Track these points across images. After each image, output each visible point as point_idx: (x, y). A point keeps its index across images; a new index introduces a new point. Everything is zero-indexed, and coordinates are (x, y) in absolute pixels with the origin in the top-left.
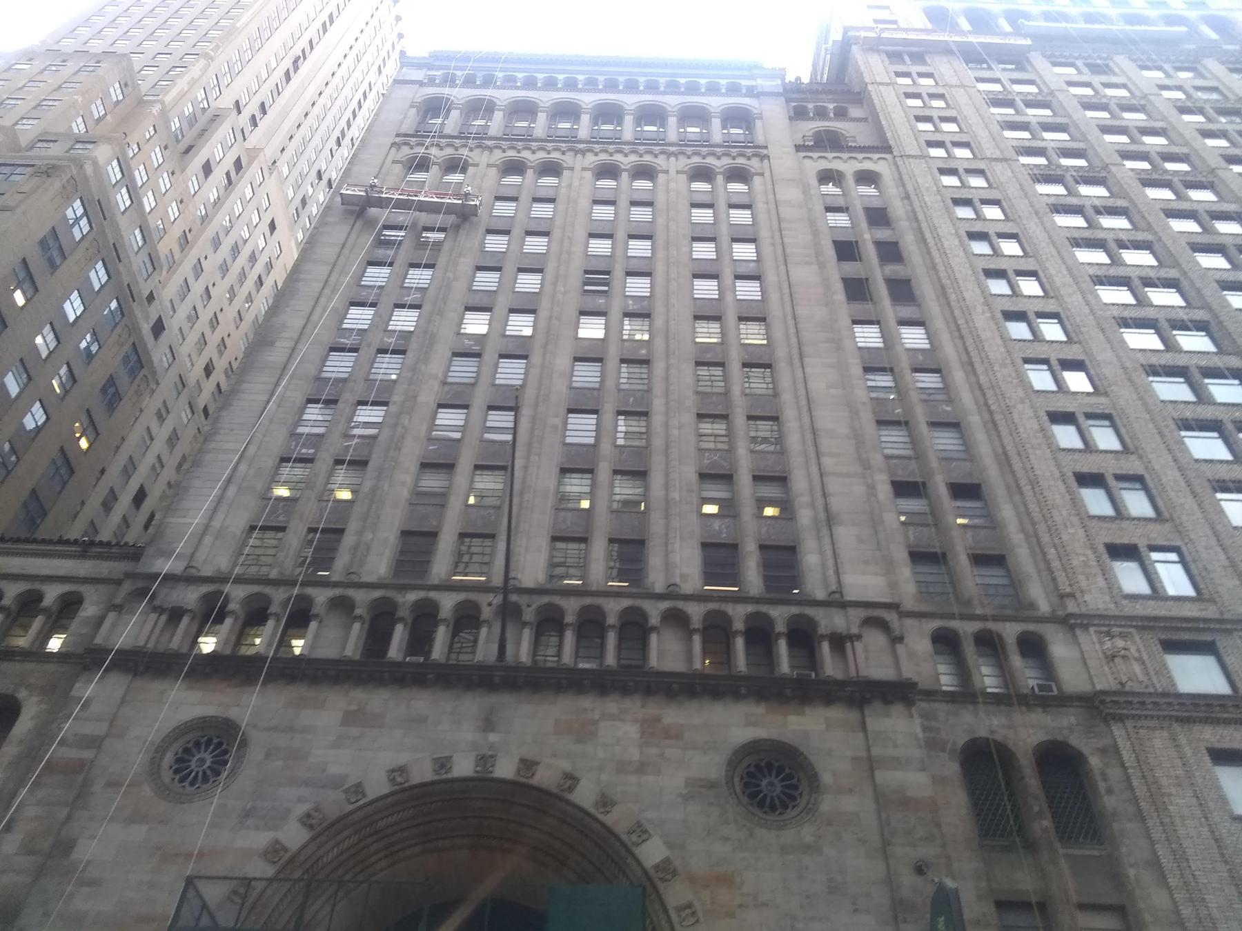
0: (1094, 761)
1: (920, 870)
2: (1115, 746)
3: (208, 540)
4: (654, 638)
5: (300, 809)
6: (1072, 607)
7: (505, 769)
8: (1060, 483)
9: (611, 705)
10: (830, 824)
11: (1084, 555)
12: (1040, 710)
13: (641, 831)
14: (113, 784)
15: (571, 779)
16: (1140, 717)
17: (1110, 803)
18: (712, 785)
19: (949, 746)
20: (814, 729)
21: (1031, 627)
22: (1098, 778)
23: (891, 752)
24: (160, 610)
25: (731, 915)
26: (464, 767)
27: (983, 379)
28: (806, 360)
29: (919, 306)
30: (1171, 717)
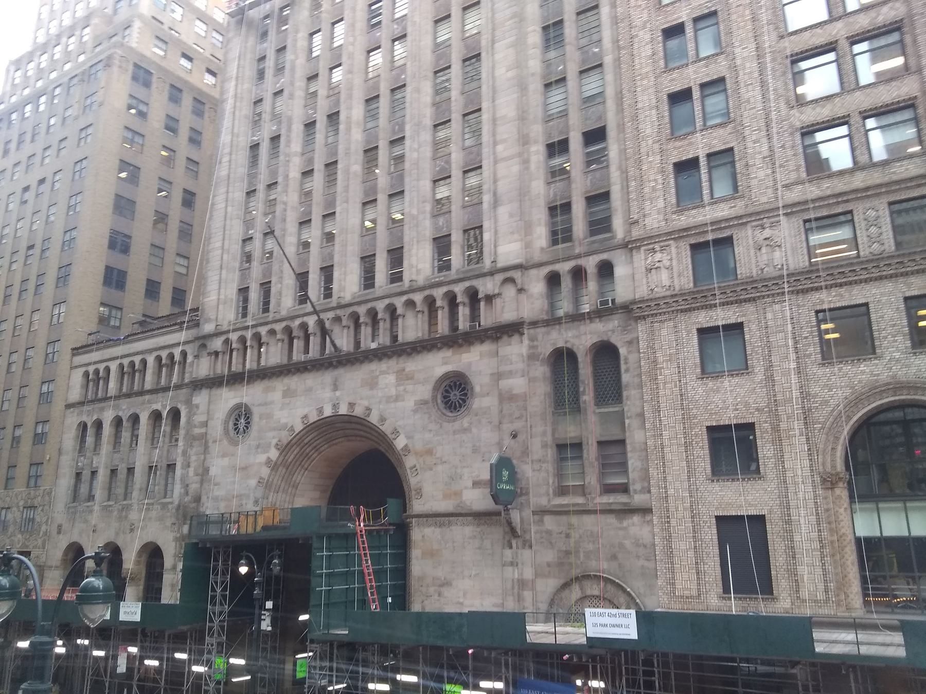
0: (623, 351)
1: (515, 436)
2: (638, 338)
3: (221, 307)
4: (400, 320)
5: (274, 441)
6: (636, 233)
7: (343, 410)
8: (654, 112)
9: (384, 365)
10: (476, 415)
11: (655, 180)
12: (598, 320)
13: (396, 432)
14: (215, 441)
15: (369, 409)
16: (656, 315)
17: (625, 378)
18: (425, 402)
19: (541, 356)
20: (474, 361)
21: (604, 256)
22: (622, 362)
23: (508, 368)
24: (209, 354)
25: (431, 469)
26: (328, 412)
28: (496, 45)
30: (677, 310)
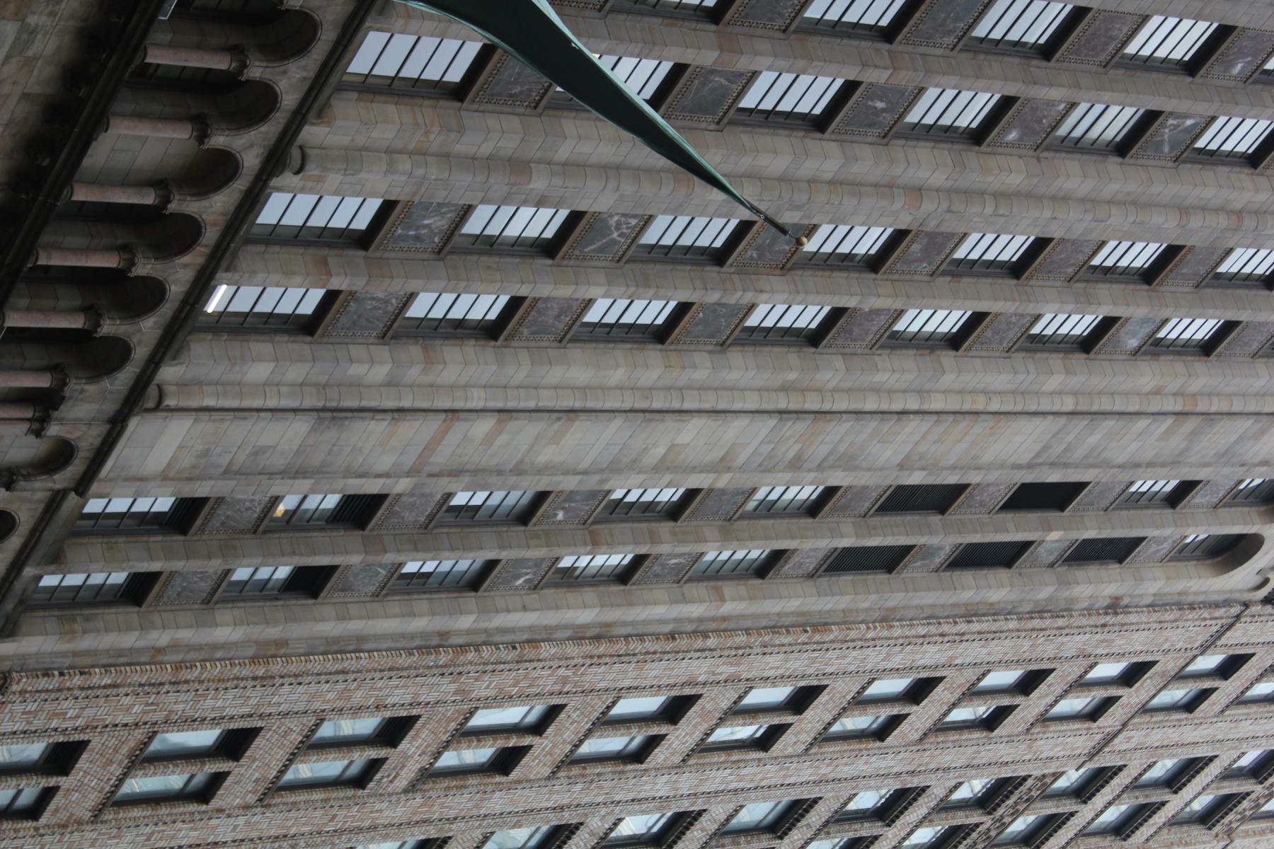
27: (547, 650)
28: (772, 422)
29: (811, 576)
